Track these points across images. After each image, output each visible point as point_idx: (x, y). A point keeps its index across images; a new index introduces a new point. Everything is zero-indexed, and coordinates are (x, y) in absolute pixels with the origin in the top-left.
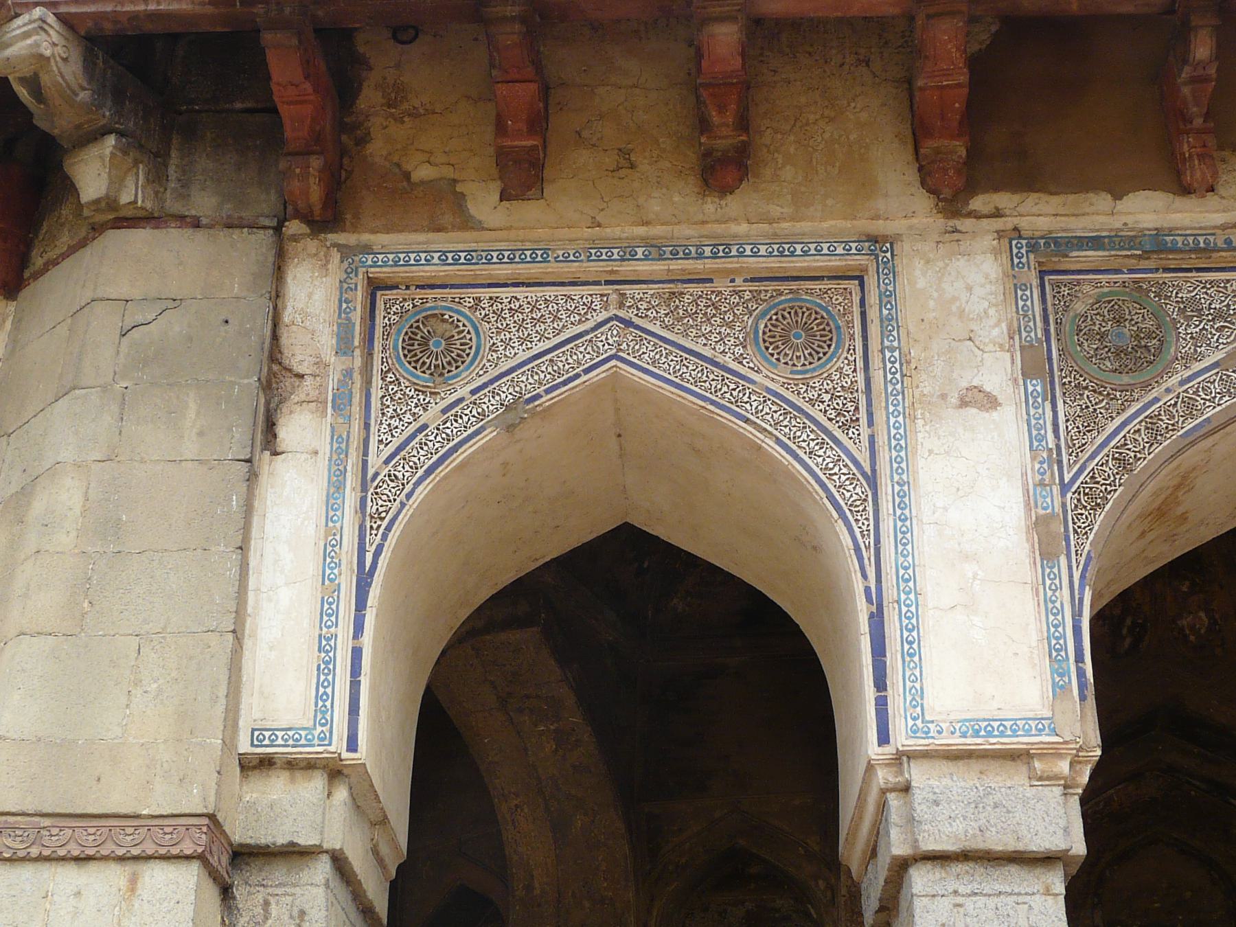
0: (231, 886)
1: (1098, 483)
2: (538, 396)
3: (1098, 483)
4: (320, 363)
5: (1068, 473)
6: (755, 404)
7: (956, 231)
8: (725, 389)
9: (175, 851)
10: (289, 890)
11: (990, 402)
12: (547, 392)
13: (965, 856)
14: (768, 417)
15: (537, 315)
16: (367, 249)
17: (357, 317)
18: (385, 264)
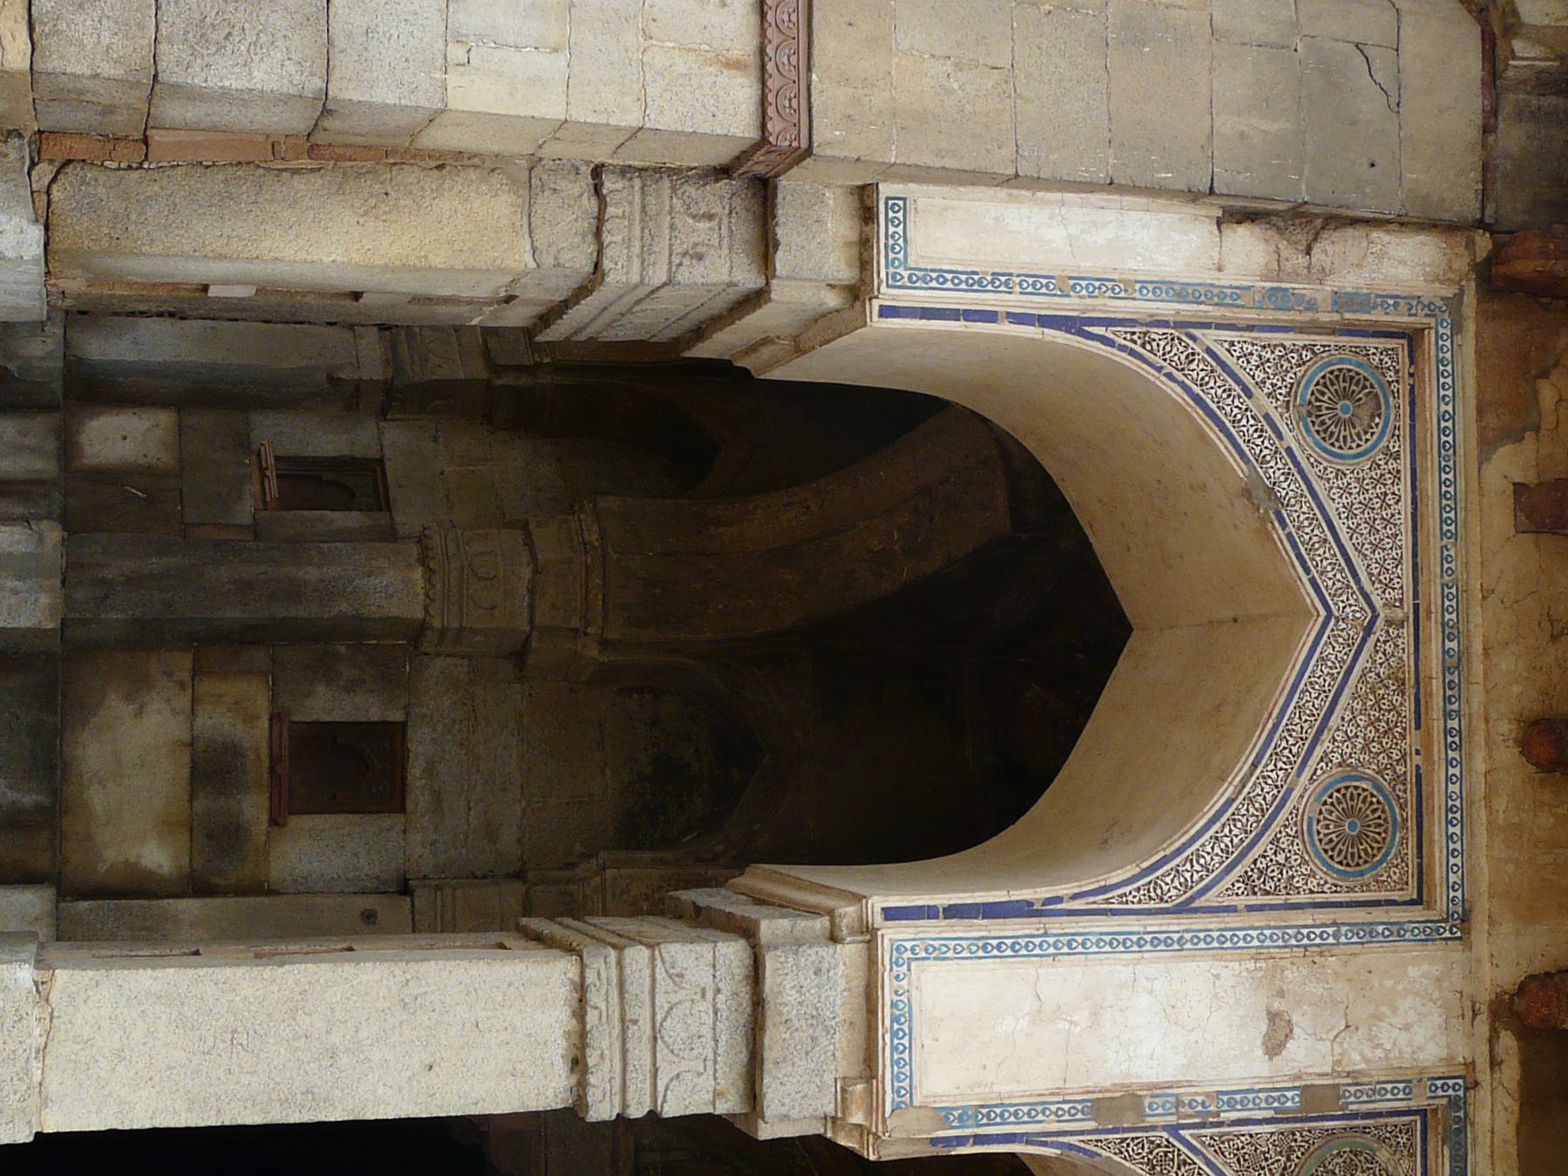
0: (730, 177)
1: (1179, 1168)
2: (1284, 525)
3: (1179, 1168)
4: (1324, 274)
5: (1191, 1135)
6: (1273, 775)
7: (1475, 1014)
8: (1291, 741)
9: (771, 111)
10: (725, 242)
11: (1274, 1048)
12: (1289, 536)
13: (758, 1001)
14: (1258, 790)
15: (1379, 525)
16: (1457, 328)
17: (1377, 316)
18: (1439, 349)
